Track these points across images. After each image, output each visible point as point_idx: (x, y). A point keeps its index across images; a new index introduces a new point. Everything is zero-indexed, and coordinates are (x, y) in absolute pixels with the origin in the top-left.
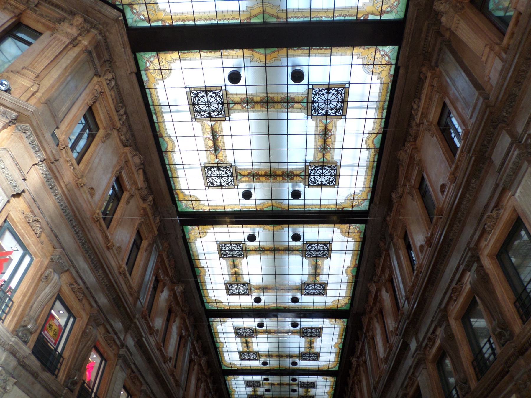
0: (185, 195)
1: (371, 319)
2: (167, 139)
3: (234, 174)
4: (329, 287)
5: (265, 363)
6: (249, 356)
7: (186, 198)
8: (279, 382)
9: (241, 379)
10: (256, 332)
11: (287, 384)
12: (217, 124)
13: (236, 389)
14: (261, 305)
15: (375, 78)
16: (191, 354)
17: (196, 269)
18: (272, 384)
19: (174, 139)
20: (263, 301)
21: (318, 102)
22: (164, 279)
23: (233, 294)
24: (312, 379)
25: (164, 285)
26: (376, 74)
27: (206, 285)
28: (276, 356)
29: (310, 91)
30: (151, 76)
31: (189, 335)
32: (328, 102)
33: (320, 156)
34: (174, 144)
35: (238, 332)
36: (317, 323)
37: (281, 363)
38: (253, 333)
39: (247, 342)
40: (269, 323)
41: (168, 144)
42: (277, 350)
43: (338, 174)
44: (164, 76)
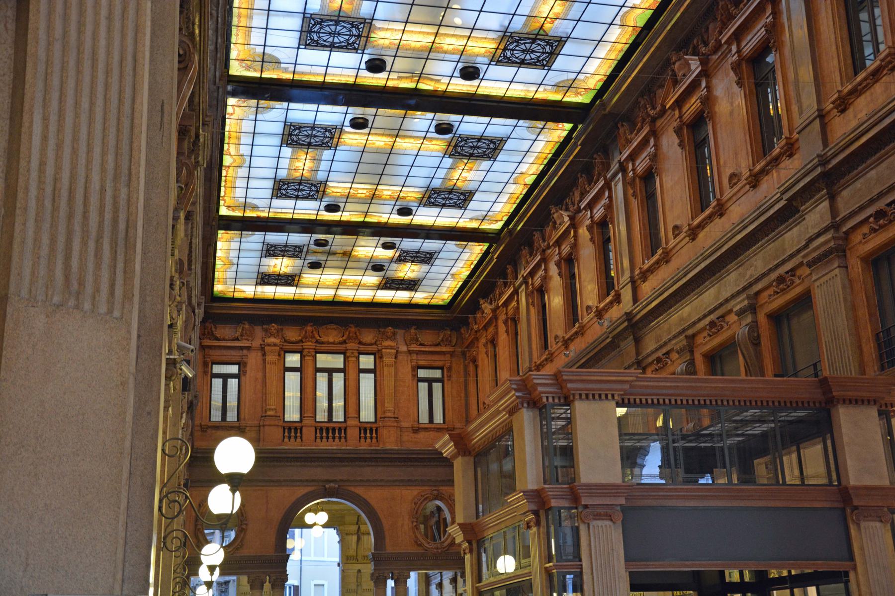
1: (654, 133)
4: (568, 48)
6: (299, 190)
14: (377, 80)
23: (316, 45)
24: (431, 245)
36: (498, 126)
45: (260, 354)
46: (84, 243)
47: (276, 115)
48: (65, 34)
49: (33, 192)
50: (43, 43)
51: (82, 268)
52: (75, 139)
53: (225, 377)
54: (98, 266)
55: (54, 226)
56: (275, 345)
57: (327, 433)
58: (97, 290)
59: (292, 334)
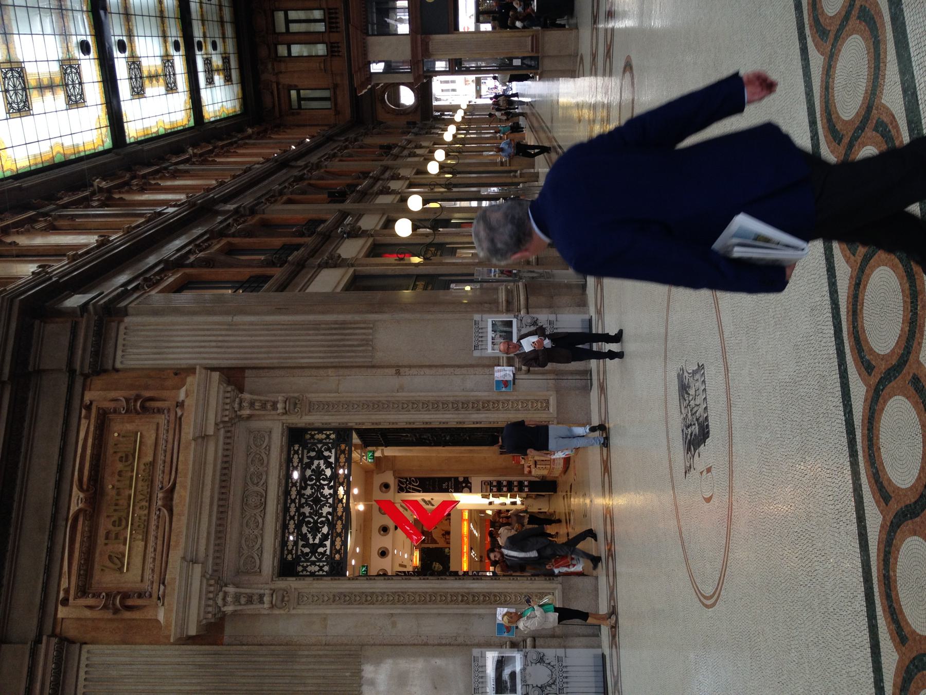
5: (177, 46)
8: (200, 22)
9: (206, 95)
10: (133, 57)
11: (201, 7)
13: (220, 105)
16: (194, 164)
17: (57, 160)
18: (205, 37)
20: (84, 38)
22: (98, 200)
23: (82, 94)
25: (110, 198)
27: (78, 145)
28: (163, 23)
31: (166, 168)
35: (138, 92)
37: (172, 15)
38: (134, 63)
39: (150, 77)
40: (116, 31)
42: (153, 19)
45: (281, 76)
46: (348, 340)
47: (130, 108)
48: (265, 353)
49: (332, 360)
50: (271, 361)
51: (357, 340)
52: (306, 346)
53: (300, 99)
54: (355, 334)
55: (343, 351)
56: (273, 65)
57: (333, 23)
58: (364, 334)
59: (263, 52)
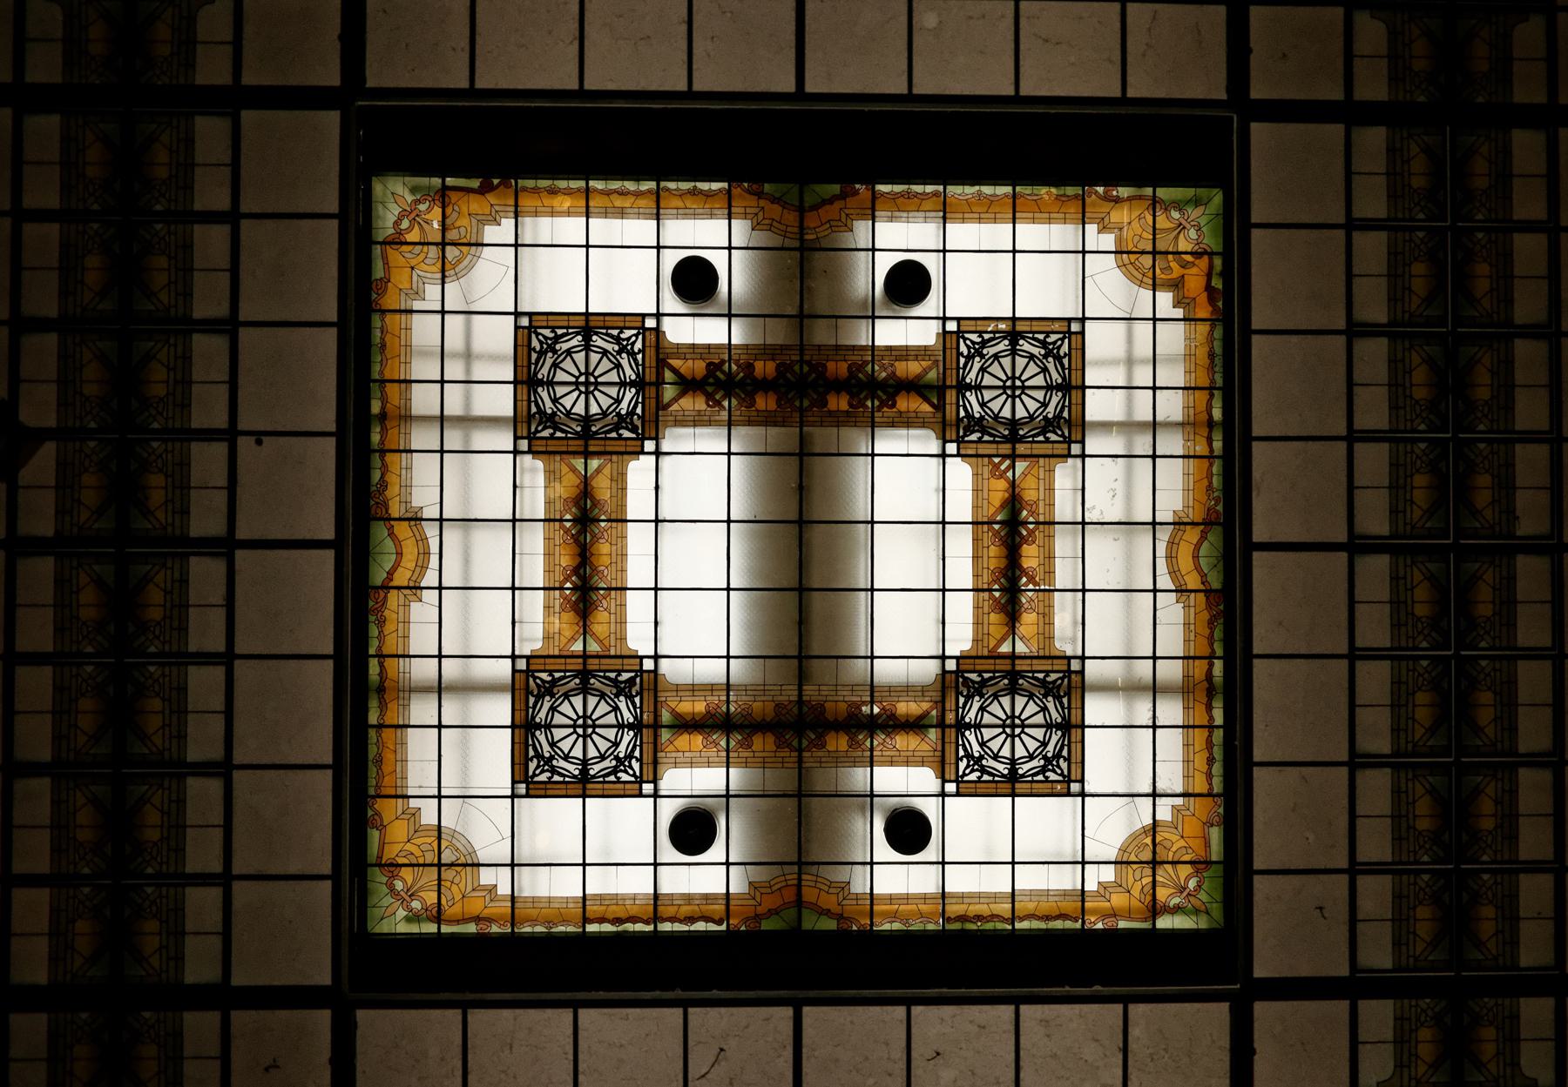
0: (1176, 285)
2: (1193, 581)
3: (951, 396)
7: (1177, 271)
12: (992, 643)
15: (429, 816)
19: (1165, 582)
21: (620, 726)
26: (428, 828)
29: (648, 775)
30: (1190, 841)
32: (585, 726)
33: (603, 488)
34: (1170, 557)
41: (1196, 557)
43: (523, 390)
44: (1148, 840)
